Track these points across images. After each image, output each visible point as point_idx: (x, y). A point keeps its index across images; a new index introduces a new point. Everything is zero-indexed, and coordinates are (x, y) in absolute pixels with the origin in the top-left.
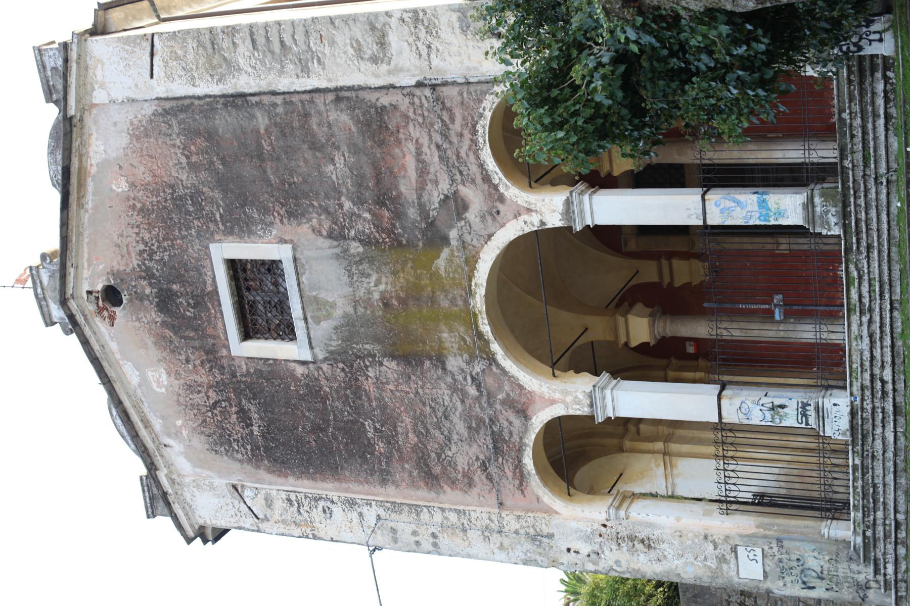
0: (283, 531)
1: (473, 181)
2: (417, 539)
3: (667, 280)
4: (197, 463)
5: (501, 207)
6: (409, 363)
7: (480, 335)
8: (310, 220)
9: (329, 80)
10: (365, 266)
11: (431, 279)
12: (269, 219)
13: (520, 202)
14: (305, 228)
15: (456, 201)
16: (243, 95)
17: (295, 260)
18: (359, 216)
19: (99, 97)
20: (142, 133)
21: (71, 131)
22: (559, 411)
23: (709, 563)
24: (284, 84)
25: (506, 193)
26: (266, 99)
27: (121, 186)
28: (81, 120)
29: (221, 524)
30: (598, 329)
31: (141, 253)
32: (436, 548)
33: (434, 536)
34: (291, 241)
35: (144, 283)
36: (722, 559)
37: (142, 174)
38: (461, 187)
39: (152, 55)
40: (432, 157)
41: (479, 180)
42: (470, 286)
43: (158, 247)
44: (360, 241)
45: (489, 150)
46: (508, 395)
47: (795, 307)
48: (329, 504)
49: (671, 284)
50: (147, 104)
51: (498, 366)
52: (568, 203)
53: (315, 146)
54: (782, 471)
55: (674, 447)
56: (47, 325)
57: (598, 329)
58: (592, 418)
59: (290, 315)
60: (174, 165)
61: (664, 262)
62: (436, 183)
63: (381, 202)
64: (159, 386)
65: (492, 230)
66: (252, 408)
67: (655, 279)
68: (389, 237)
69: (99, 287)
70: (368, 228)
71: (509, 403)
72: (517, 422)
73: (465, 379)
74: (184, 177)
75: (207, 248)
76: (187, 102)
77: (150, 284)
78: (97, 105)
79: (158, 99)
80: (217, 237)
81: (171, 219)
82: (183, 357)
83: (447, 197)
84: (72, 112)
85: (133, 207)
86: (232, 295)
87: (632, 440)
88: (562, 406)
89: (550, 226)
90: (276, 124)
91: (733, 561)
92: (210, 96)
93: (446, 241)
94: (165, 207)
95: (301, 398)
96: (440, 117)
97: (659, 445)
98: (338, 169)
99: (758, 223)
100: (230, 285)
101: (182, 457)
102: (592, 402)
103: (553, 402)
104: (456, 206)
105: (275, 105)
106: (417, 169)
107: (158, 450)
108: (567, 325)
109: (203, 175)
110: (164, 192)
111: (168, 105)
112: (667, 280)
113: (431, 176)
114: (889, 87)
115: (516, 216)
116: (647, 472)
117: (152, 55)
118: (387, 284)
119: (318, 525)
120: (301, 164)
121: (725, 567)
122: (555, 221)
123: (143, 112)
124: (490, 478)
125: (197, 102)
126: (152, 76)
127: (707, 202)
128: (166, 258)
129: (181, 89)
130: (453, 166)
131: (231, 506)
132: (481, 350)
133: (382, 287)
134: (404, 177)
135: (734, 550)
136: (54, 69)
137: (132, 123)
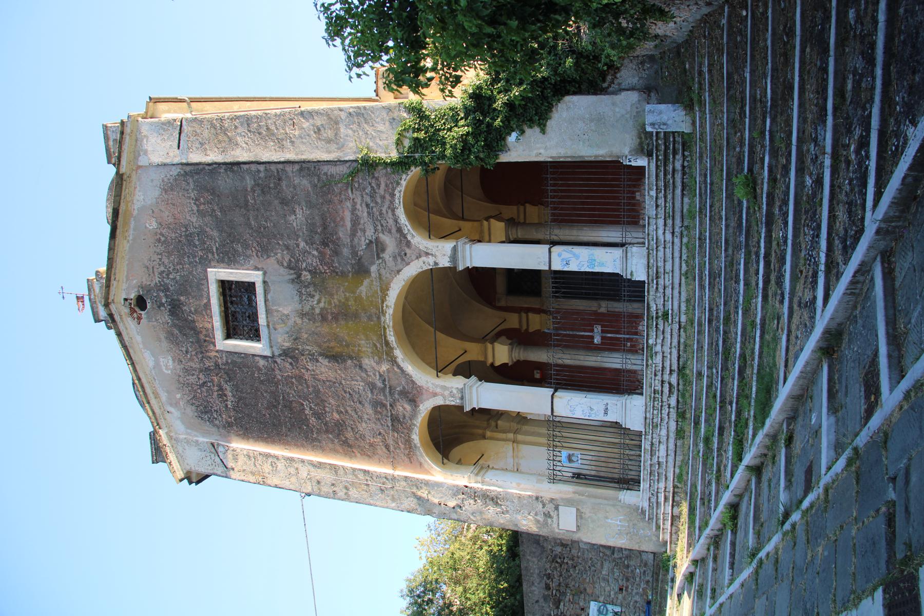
0: (244, 478)
1: (390, 232)
2: (335, 489)
3: (524, 327)
4: (189, 426)
5: (408, 251)
6: (337, 361)
7: (387, 343)
8: (276, 254)
9: (297, 154)
10: (311, 289)
11: (355, 301)
12: (249, 252)
14: (272, 260)
15: (377, 245)
16: (238, 164)
17: (265, 282)
18: (309, 253)
19: (143, 161)
20: (168, 188)
22: (439, 401)
23: (538, 518)
24: (266, 156)
26: (253, 167)
27: (153, 225)
29: (203, 470)
30: (474, 352)
31: (161, 273)
32: (347, 498)
33: (346, 488)
34: (262, 269)
35: (162, 294)
36: (547, 515)
37: (167, 217)
38: (381, 235)
39: (180, 134)
40: (363, 213)
41: (394, 230)
43: (174, 269)
44: (310, 271)
46: (404, 388)
47: (609, 335)
48: (275, 460)
49: (527, 330)
50: (174, 168)
51: (399, 367)
52: (455, 249)
53: (284, 202)
54: (594, 458)
55: (520, 437)
56: (96, 321)
57: (474, 352)
58: (461, 408)
59: (258, 322)
60: (188, 213)
61: (524, 315)
62: (364, 231)
63: (325, 244)
65: (401, 267)
66: (228, 388)
67: (517, 326)
69: (133, 296)
70: (315, 262)
71: (404, 393)
72: (408, 407)
73: (375, 375)
74: (194, 220)
75: (206, 271)
76: (201, 167)
77: (166, 296)
78: (141, 167)
79: (182, 164)
80: (213, 264)
81: (184, 250)
82: (184, 349)
83: (371, 242)
84: (122, 170)
85: (159, 240)
87: (492, 431)
89: (441, 266)
90: (258, 185)
91: (555, 517)
92: (216, 163)
93: (367, 272)
94: (180, 241)
95: (262, 382)
96: (370, 184)
97: (511, 436)
98: (299, 218)
99: (588, 270)
101: (178, 421)
103: (435, 395)
104: (378, 247)
105: (259, 171)
106: (351, 221)
107: (163, 414)
108: (451, 347)
109: (208, 219)
111: (188, 169)
112: (524, 327)
113: (361, 226)
114: (686, 164)
115: (418, 257)
116: (499, 449)
117: (180, 134)
120: (273, 214)
121: (549, 520)
122: (445, 263)
124: (387, 447)
125: (207, 167)
128: (178, 278)
130: (377, 219)
132: (387, 354)
133: (322, 305)
134: (343, 226)
135: (557, 508)
136: (115, 140)
137: (163, 181)
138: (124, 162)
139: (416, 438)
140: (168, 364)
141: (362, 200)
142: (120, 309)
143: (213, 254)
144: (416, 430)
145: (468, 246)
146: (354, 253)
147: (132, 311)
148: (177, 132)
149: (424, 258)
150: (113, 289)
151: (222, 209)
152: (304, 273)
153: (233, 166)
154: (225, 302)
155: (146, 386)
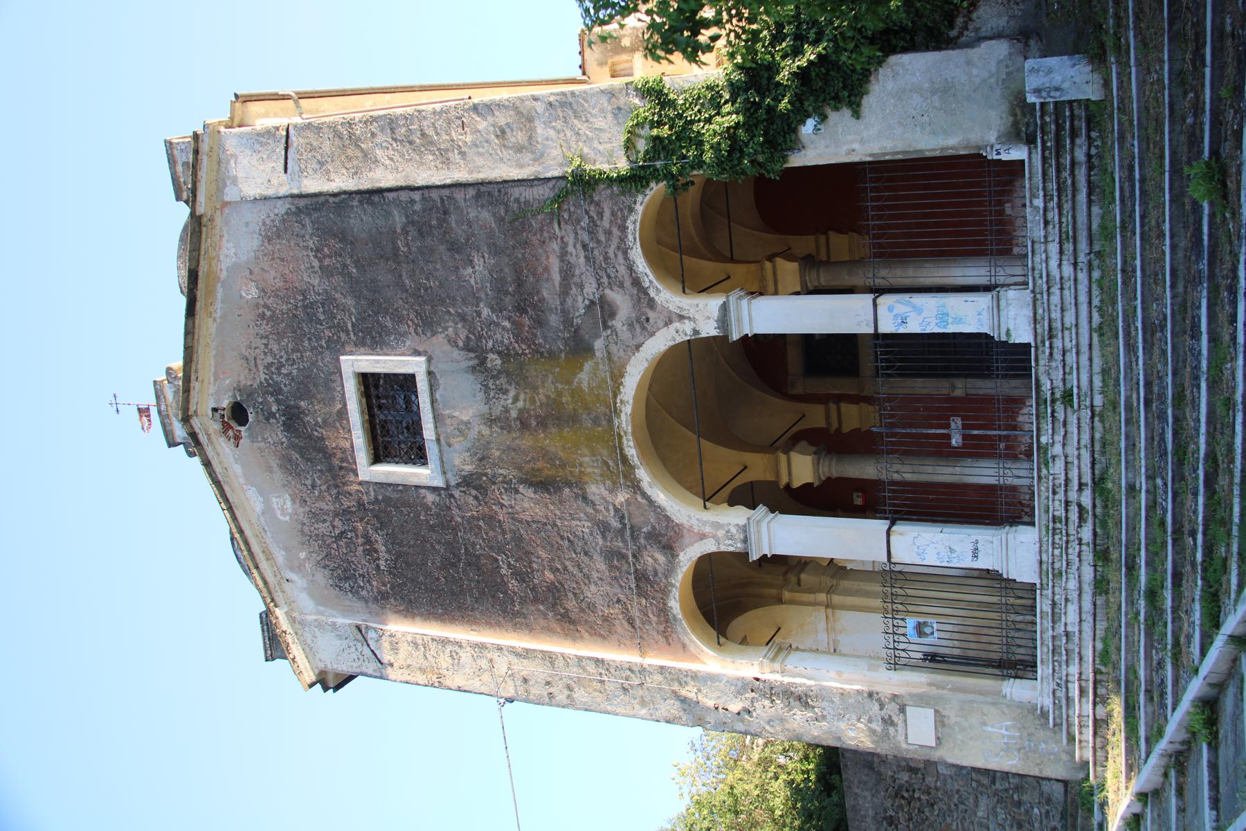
1: (621, 285)
2: (551, 690)
3: (835, 425)
4: (321, 601)
5: (651, 314)
7: (625, 459)
8: (446, 329)
9: (471, 172)
11: (572, 396)
12: (403, 328)
13: (671, 308)
14: (440, 338)
15: (602, 307)
16: (380, 191)
18: (497, 325)
19: (231, 194)
20: (272, 234)
21: (200, 232)
22: (710, 547)
23: (873, 726)
24: (423, 177)
25: (656, 298)
26: (404, 196)
27: (251, 293)
28: (211, 220)
29: (345, 668)
30: (758, 467)
32: (571, 704)
33: (569, 688)
35: (270, 399)
36: (888, 722)
37: (273, 278)
38: (608, 291)
39: (286, 149)
41: (628, 283)
42: (615, 403)
44: (499, 353)
45: (639, 249)
46: (654, 528)
47: (975, 432)
49: (839, 429)
50: (280, 202)
51: (644, 495)
52: (724, 308)
53: (454, 248)
55: (836, 599)
56: (170, 445)
57: (758, 467)
58: (744, 556)
61: (833, 407)
64: (283, 514)
65: (641, 339)
66: (379, 539)
67: (822, 424)
68: (529, 347)
69: (225, 403)
70: (507, 338)
71: (654, 536)
72: (661, 558)
73: (607, 509)
74: (316, 282)
75: (338, 360)
76: (322, 199)
77: (278, 402)
78: (229, 203)
79: (292, 196)
80: (348, 349)
81: (301, 328)
82: (309, 482)
83: (592, 302)
85: (263, 316)
86: (362, 413)
87: (792, 591)
88: (713, 541)
89: (703, 335)
90: (413, 223)
92: (345, 192)
93: (589, 350)
94: (295, 316)
95: (431, 528)
96: (587, 213)
97: (822, 597)
98: (478, 271)
100: (361, 402)
101: (303, 596)
102: (746, 537)
103: (703, 536)
105: (412, 201)
106: (561, 272)
107: (280, 585)
108: (724, 462)
109: (337, 279)
110: (295, 298)
112: (835, 425)
113: (576, 279)
114: (1093, 151)
115: (668, 323)
116: (806, 620)
117: (286, 149)
118: (525, 401)
119: (445, 672)
121: (892, 730)
122: (709, 329)
123: (276, 211)
124: (631, 621)
125: (331, 200)
126: (286, 171)
127: (879, 308)
128: (295, 372)
129: (313, 185)
130: (601, 268)
131: (353, 649)
132: (625, 477)
133: (520, 404)
134: (547, 280)
135: (902, 710)
136: (185, 164)
137: (264, 224)
138: (201, 197)
139: (675, 605)
140: (284, 506)
141: (576, 238)
142: (207, 425)
143: (348, 333)
144: (675, 593)
145: (745, 302)
146: (568, 322)
147: (226, 427)
148: (282, 146)
149: (676, 325)
150: (194, 396)
151: (357, 263)
152: (491, 356)
153: (373, 195)
154: (370, 407)
155: (252, 541)
